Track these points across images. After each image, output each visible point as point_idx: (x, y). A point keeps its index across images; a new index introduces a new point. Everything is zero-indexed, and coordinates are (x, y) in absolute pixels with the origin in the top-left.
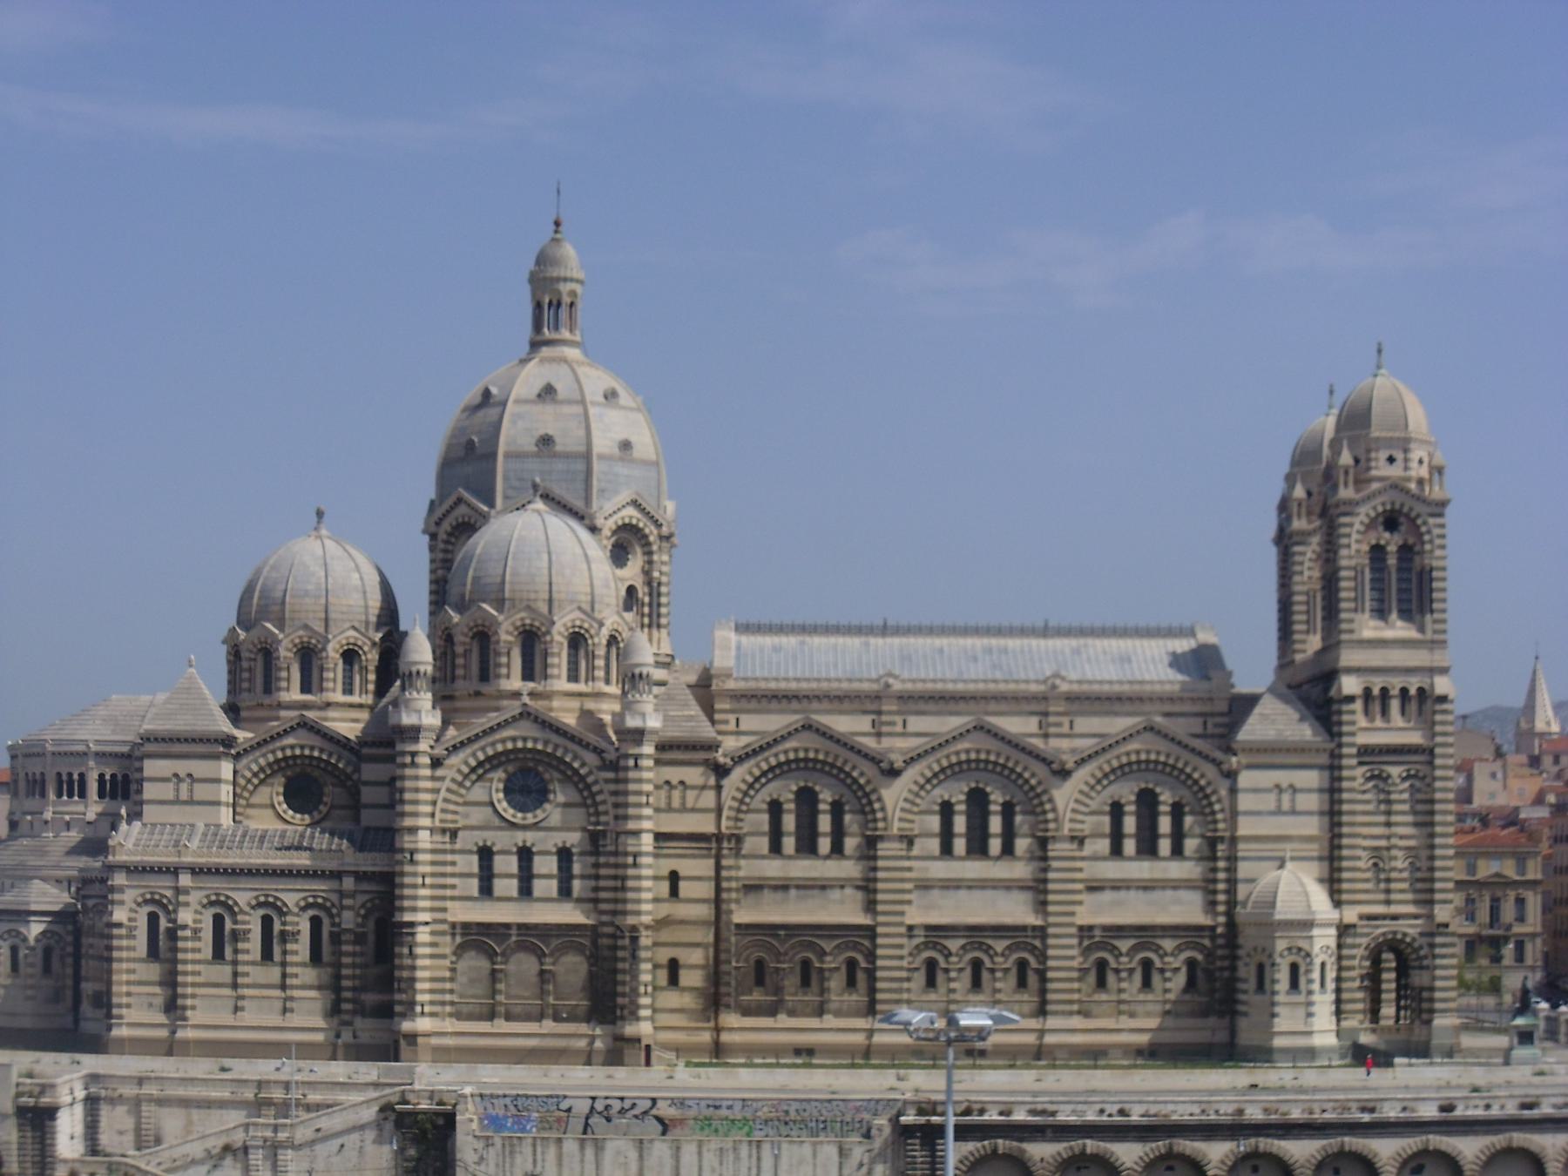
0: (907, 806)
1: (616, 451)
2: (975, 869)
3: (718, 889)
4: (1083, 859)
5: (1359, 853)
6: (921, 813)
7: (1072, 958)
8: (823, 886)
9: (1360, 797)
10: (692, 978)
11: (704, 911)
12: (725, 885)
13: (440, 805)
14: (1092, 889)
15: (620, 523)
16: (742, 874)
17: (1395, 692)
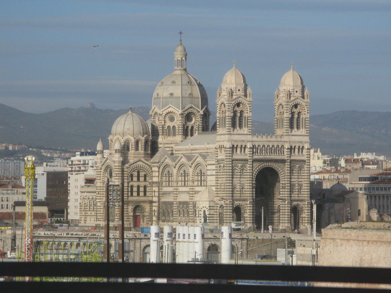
0: (176, 175)
1: (169, 96)
2: (184, 189)
3: (159, 194)
4: (194, 186)
5: (218, 184)
6: (178, 176)
7: (192, 209)
8: (169, 193)
9: (218, 171)
10: (156, 214)
11: (155, 199)
12: (160, 193)
13: (102, 177)
14: (195, 193)
15: (168, 112)
16: (162, 190)
17: (222, 146)
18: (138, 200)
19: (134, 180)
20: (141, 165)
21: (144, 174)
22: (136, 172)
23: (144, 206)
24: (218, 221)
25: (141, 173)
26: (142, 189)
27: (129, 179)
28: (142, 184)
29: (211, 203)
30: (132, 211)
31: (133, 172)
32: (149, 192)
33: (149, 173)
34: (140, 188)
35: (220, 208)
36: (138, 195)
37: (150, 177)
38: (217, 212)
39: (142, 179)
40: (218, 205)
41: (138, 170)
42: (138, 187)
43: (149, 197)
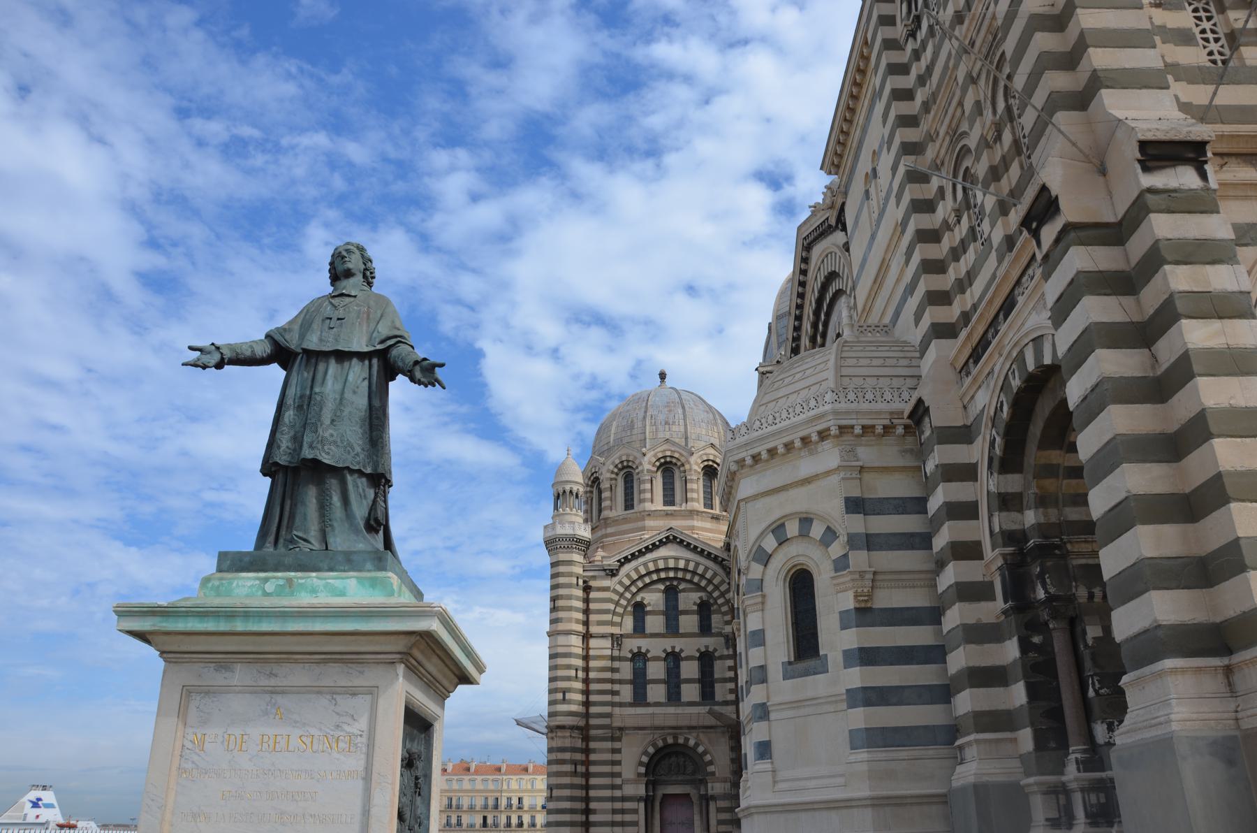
18: (658, 722)
19: (648, 631)
20: (677, 559)
21: (698, 601)
22: (659, 591)
23: (701, 749)
24: (1017, 695)
25: (681, 596)
26: (690, 669)
27: (620, 625)
28: (690, 646)
29: (867, 454)
30: (639, 775)
31: (640, 590)
32: (725, 680)
33: (719, 597)
34: (683, 664)
35: (1009, 461)
36: (674, 696)
37: (724, 614)
38: (967, 551)
39: (689, 623)
40: (976, 452)
41: (668, 583)
42: (673, 658)
43: (726, 703)
